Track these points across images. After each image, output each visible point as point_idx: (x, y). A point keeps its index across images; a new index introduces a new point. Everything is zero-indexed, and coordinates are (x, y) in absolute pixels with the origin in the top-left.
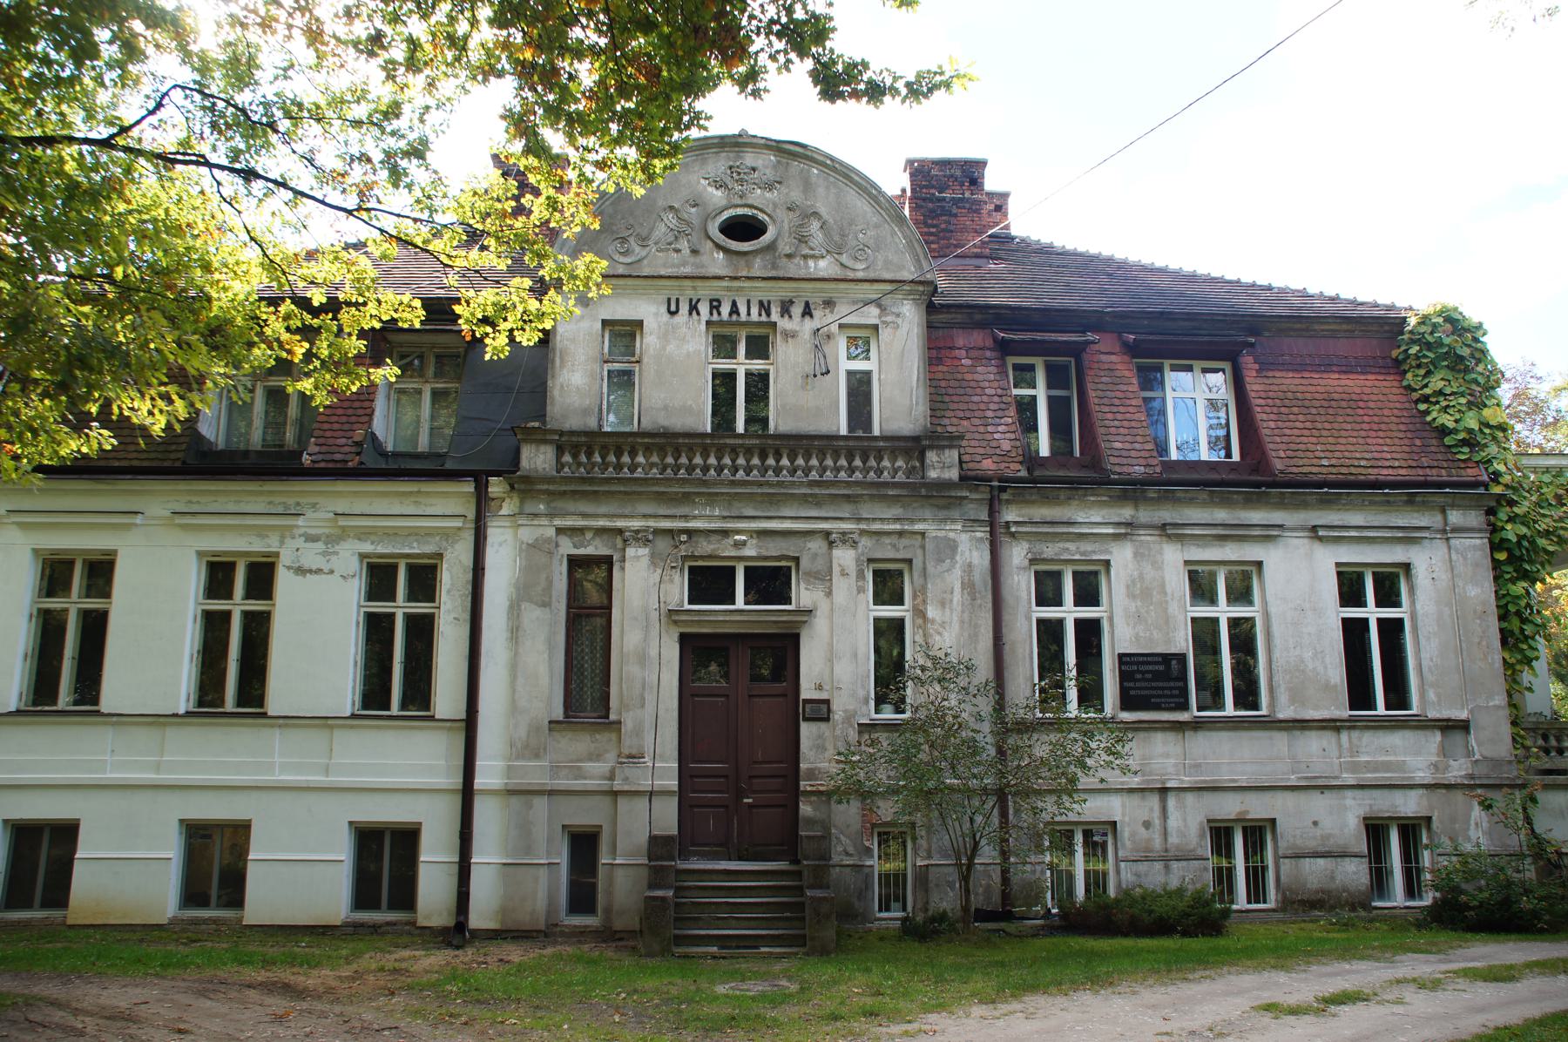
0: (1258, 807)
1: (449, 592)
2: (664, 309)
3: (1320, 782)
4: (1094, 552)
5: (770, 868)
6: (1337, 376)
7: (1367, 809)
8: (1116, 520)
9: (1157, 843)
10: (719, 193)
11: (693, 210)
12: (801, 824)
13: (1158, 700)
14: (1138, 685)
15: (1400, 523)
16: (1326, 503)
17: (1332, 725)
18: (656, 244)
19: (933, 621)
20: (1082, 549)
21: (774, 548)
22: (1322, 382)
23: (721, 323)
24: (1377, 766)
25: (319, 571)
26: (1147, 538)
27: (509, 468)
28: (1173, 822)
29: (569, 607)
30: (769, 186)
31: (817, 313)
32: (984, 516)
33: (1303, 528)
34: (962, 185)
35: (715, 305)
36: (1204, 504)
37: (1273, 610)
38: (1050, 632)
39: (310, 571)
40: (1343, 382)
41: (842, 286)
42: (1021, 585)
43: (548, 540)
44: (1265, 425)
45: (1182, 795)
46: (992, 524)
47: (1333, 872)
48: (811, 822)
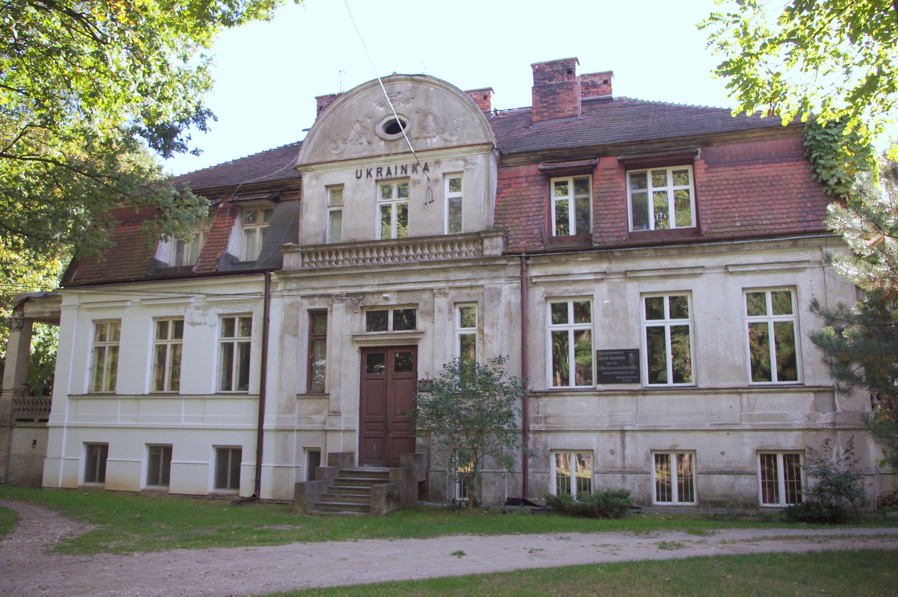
0: (684, 442)
1: (255, 330)
2: (354, 176)
3: (726, 427)
4: (584, 291)
5: (376, 471)
6: (761, 166)
7: (759, 445)
8: (597, 270)
9: (619, 463)
10: (382, 109)
11: (369, 120)
12: (416, 448)
13: (621, 377)
14: (608, 368)
15: (790, 259)
16: (734, 250)
17: (736, 391)
18: (351, 141)
19: (487, 335)
20: (576, 290)
21: (406, 299)
22: (749, 171)
23: (382, 180)
24: (765, 417)
25: (200, 324)
26: (615, 280)
27: (278, 267)
28: (629, 451)
29: (310, 336)
30: (407, 101)
31: (431, 169)
32: (518, 274)
33: (719, 267)
34: (563, 74)
35: (379, 170)
36: (652, 257)
37: (698, 320)
38: (560, 338)
39: (197, 324)
40: (764, 170)
41: (443, 152)
42: (541, 314)
43: (297, 303)
44: (702, 203)
45: (635, 434)
46: (522, 278)
47: (733, 484)
48: (421, 446)
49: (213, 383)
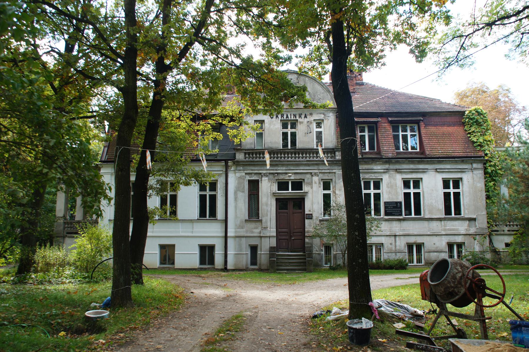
0: (419, 240)
3: (436, 234)
12: (306, 244)
16: (440, 162)
17: (440, 219)
19: (337, 194)
21: (298, 177)
23: (284, 120)
24: (451, 230)
26: (392, 172)
28: (398, 244)
29: (249, 192)
36: (407, 164)
37: (425, 190)
40: (447, 129)
43: (243, 176)
48: (308, 243)
49: (195, 213)
